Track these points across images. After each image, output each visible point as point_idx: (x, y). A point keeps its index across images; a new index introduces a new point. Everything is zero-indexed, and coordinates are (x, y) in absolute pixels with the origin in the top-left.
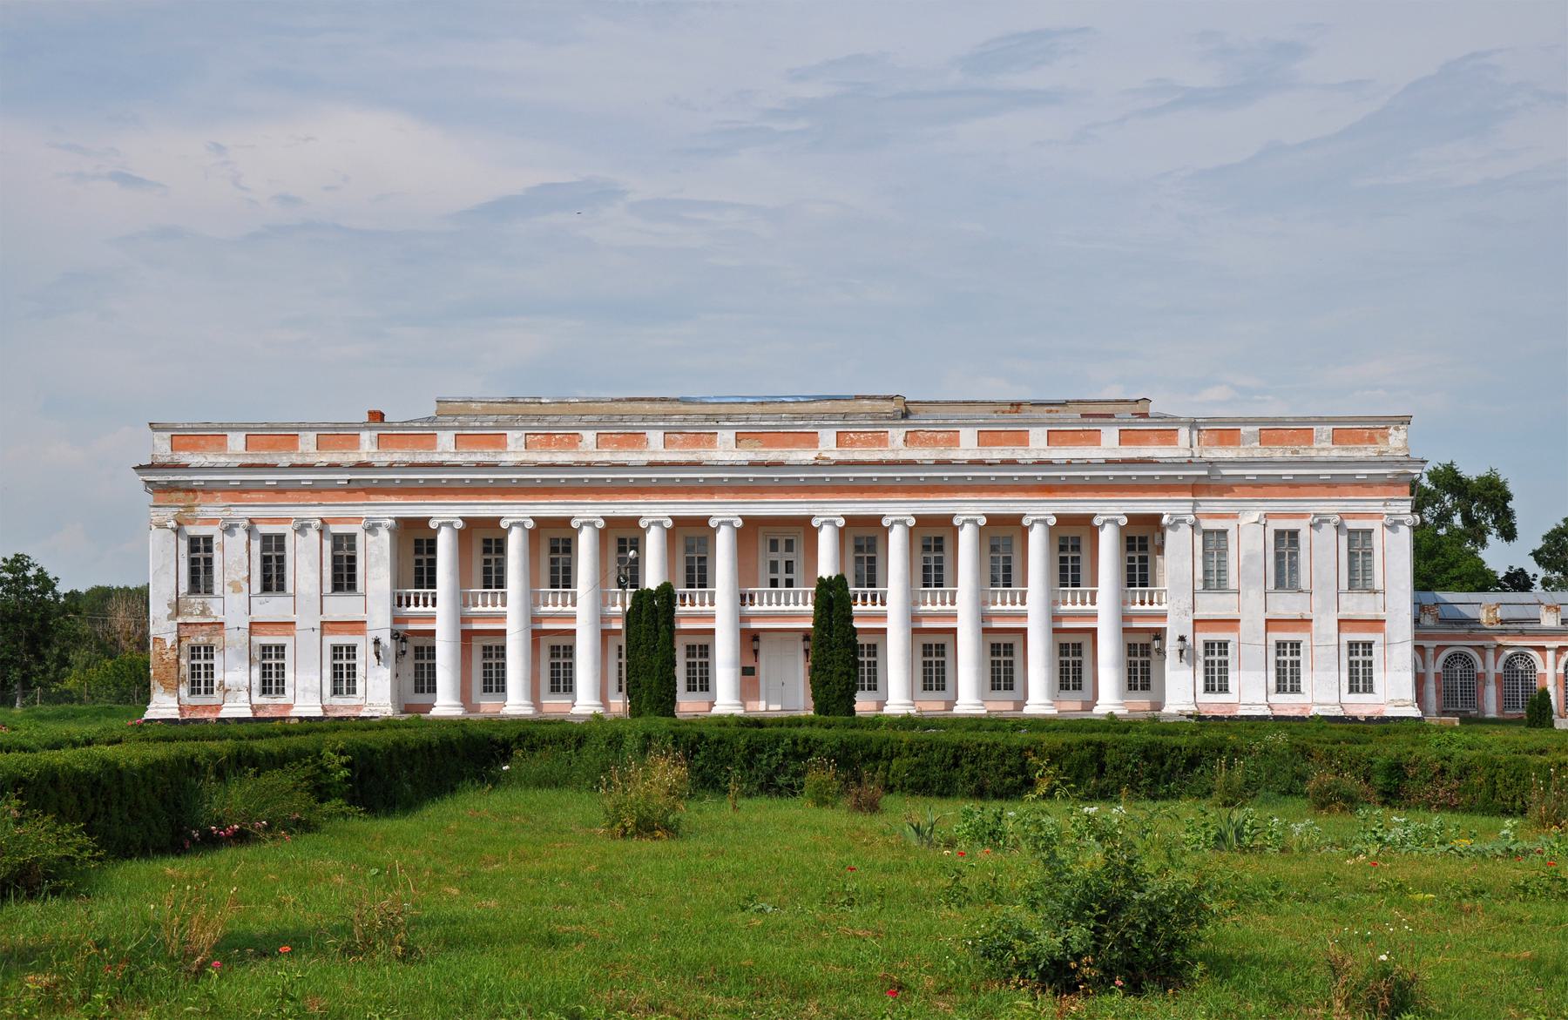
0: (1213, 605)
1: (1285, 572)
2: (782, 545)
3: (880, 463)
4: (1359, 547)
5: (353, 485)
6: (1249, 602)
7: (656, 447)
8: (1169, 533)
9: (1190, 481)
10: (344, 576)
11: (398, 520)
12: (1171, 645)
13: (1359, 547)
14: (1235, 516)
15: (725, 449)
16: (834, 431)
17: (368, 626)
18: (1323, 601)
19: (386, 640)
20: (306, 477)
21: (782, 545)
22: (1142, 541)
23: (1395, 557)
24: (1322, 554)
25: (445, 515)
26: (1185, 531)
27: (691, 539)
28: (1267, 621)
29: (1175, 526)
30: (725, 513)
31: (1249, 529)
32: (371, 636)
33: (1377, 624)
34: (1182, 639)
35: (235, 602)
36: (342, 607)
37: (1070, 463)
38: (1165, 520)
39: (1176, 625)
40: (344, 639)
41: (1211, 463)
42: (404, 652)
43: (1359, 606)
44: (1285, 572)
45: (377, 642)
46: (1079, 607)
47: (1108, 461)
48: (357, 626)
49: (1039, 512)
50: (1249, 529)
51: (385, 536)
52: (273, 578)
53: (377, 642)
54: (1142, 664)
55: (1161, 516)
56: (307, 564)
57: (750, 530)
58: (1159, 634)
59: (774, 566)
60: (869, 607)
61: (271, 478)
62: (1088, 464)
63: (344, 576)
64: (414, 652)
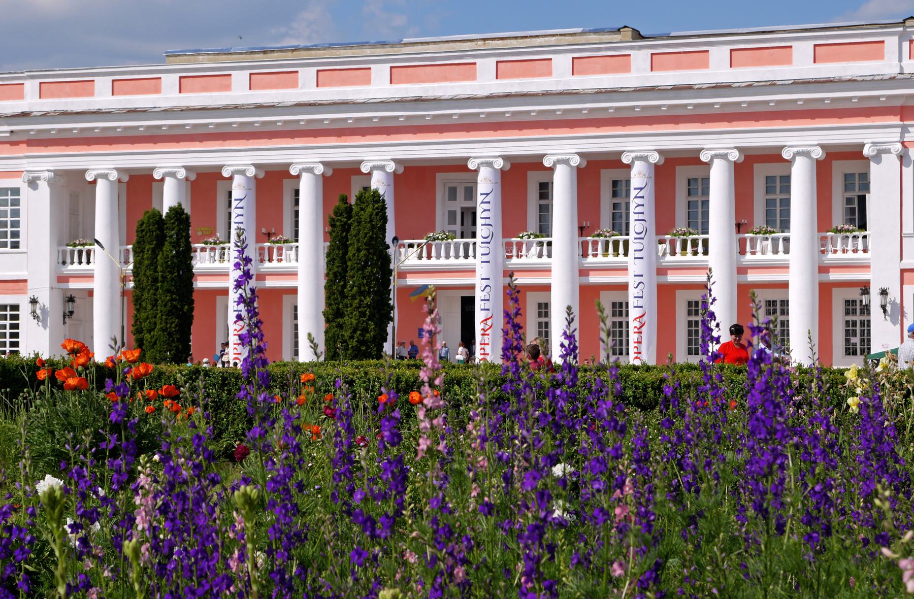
2: (460, 194)
3: (546, 96)
5: (15, 138)
8: (873, 165)
9: (898, 103)
11: (56, 172)
12: (875, 300)
16: (493, 60)
17: (30, 285)
19: (45, 299)
21: (460, 194)
26: (891, 161)
28: (903, 271)
29: (878, 158)
32: (30, 295)
34: (884, 292)
37: (750, 87)
38: (866, 151)
42: (71, 313)
45: (34, 301)
46: (850, 255)
47: (796, 83)
51: (44, 189)
53: (34, 301)
54: (862, 323)
55: (862, 145)
57: (415, 177)
58: (865, 287)
59: (452, 214)
60: (689, 257)
62: (771, 86)
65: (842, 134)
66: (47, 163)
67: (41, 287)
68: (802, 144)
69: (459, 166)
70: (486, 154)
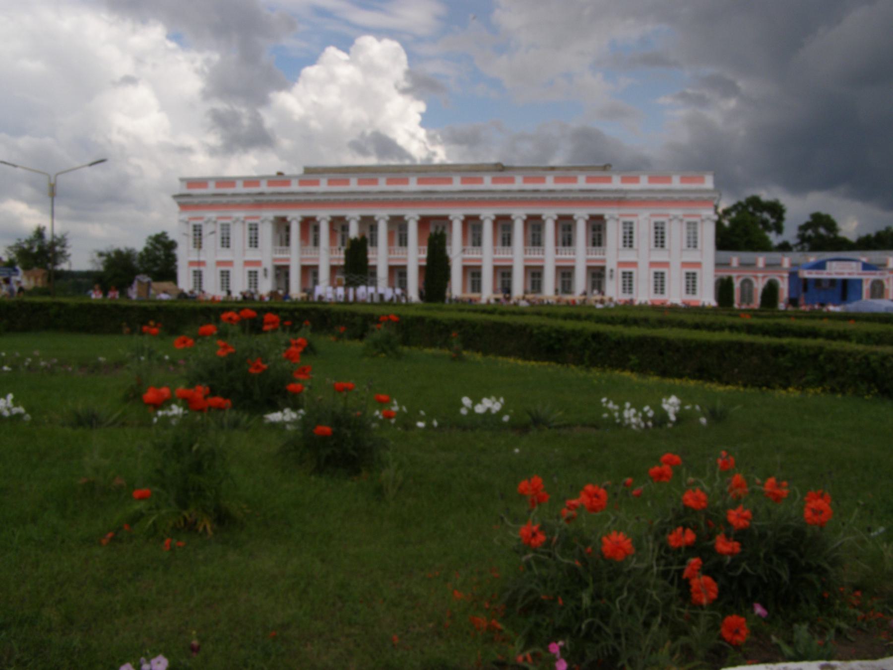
0: (628, 256)
1: (660, 239)
4: (692, 227)
6: (644, 253)
7: (382, 185)
10: (254, 242)
13: (692, 227)
14: (636, 215)
15: (413, 185)
18: (676, 253)
20: (238, 199)
22: (597, 226)
23: (708, 235)
24: (676, 235)
25: (294, 216)
27: (369, 223)
30: (412, 215)
31: (644, 222)
33: (698, 265)
34: (612, 271)
35: (212, 252)
36: (252, 255)
37: (562, 191)
39: (611, 264)
40: (253, 268)
41: (627, 192)
43: (691, 256)
44: (660, 239)
48: (258, 263)
49: (550, 214)
50: (644, 222)
52: (226, 242)
53: (265, 270)
56: (239, 235)
57: (424, 222)
58: (603, 269)
61: (224, 200)
62: (570, 191)
63: (254, 242)
64: (282, 272)
65: (596, 211)
66: (270, 214)
67: (268, 264)
68: (581, 214)
69: (445, 218)
70: (457, 215)
